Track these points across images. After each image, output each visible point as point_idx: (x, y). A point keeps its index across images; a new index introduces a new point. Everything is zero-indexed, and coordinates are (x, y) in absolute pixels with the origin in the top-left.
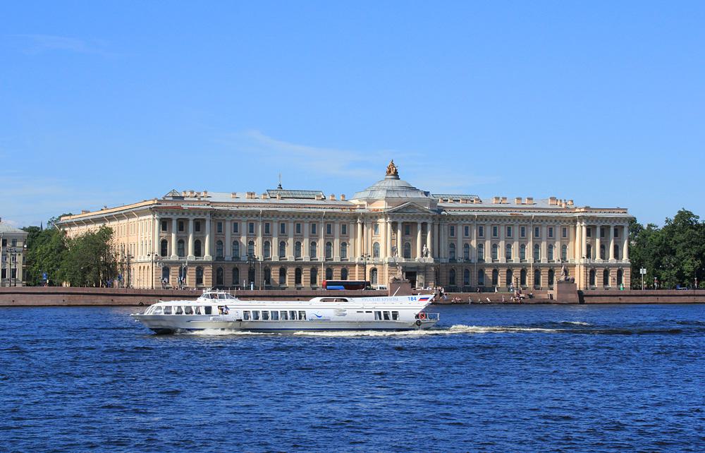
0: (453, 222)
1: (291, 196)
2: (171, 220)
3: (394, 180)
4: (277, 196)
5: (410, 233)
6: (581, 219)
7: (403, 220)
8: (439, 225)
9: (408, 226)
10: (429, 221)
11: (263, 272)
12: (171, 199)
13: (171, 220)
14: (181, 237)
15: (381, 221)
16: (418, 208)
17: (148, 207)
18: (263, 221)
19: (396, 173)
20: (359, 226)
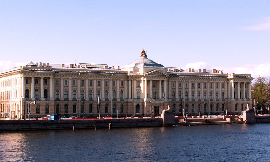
0: (174, 80)
1: (94, 67)
2: (31, 78)
3: (144, 59)
4: (86, 67)
5: (156, 86)
6: (231, 79)
7: (153, 79)
8: (168, 82)
9: (155, 82)
10: (165, 79)
11: (81, 106)
12: (30, 66)
13: (31, 78)
14: (27, 87)
15: (142, 79)
16: (160, 73)
17: (18, 71)
18: (81, 79)
19: (146, 56)
20: (130, 82)
